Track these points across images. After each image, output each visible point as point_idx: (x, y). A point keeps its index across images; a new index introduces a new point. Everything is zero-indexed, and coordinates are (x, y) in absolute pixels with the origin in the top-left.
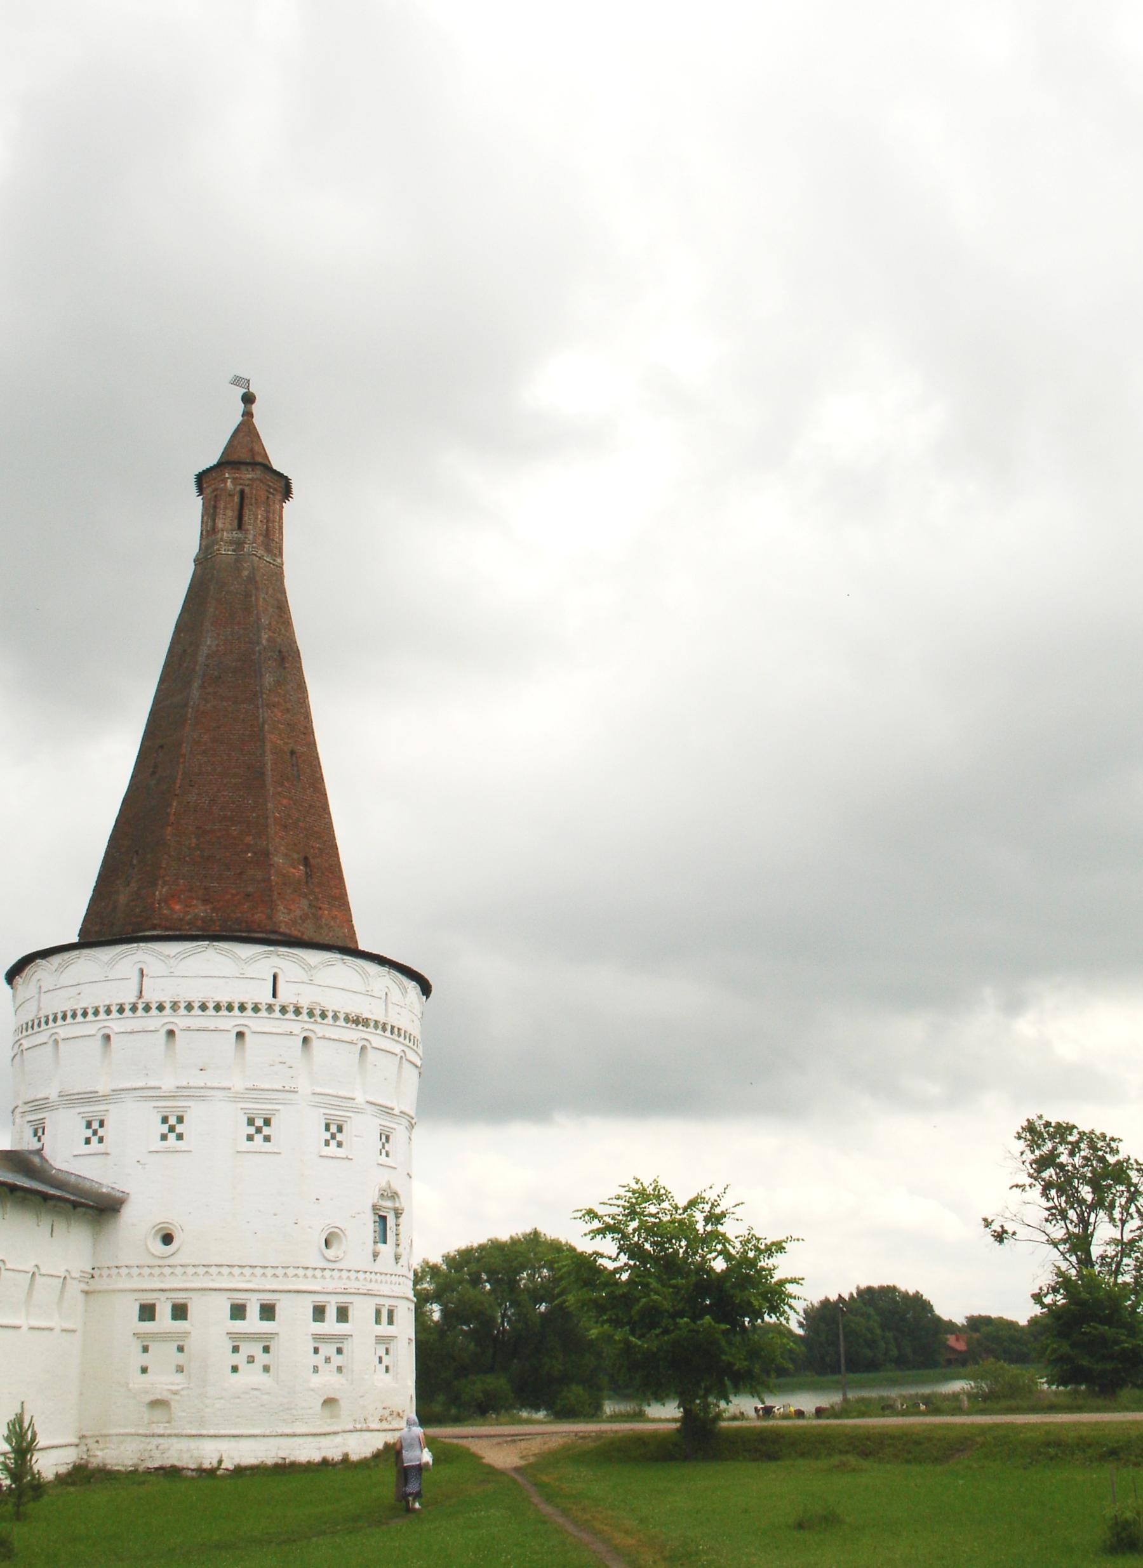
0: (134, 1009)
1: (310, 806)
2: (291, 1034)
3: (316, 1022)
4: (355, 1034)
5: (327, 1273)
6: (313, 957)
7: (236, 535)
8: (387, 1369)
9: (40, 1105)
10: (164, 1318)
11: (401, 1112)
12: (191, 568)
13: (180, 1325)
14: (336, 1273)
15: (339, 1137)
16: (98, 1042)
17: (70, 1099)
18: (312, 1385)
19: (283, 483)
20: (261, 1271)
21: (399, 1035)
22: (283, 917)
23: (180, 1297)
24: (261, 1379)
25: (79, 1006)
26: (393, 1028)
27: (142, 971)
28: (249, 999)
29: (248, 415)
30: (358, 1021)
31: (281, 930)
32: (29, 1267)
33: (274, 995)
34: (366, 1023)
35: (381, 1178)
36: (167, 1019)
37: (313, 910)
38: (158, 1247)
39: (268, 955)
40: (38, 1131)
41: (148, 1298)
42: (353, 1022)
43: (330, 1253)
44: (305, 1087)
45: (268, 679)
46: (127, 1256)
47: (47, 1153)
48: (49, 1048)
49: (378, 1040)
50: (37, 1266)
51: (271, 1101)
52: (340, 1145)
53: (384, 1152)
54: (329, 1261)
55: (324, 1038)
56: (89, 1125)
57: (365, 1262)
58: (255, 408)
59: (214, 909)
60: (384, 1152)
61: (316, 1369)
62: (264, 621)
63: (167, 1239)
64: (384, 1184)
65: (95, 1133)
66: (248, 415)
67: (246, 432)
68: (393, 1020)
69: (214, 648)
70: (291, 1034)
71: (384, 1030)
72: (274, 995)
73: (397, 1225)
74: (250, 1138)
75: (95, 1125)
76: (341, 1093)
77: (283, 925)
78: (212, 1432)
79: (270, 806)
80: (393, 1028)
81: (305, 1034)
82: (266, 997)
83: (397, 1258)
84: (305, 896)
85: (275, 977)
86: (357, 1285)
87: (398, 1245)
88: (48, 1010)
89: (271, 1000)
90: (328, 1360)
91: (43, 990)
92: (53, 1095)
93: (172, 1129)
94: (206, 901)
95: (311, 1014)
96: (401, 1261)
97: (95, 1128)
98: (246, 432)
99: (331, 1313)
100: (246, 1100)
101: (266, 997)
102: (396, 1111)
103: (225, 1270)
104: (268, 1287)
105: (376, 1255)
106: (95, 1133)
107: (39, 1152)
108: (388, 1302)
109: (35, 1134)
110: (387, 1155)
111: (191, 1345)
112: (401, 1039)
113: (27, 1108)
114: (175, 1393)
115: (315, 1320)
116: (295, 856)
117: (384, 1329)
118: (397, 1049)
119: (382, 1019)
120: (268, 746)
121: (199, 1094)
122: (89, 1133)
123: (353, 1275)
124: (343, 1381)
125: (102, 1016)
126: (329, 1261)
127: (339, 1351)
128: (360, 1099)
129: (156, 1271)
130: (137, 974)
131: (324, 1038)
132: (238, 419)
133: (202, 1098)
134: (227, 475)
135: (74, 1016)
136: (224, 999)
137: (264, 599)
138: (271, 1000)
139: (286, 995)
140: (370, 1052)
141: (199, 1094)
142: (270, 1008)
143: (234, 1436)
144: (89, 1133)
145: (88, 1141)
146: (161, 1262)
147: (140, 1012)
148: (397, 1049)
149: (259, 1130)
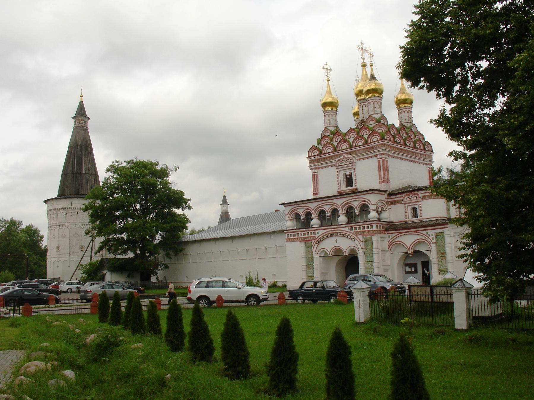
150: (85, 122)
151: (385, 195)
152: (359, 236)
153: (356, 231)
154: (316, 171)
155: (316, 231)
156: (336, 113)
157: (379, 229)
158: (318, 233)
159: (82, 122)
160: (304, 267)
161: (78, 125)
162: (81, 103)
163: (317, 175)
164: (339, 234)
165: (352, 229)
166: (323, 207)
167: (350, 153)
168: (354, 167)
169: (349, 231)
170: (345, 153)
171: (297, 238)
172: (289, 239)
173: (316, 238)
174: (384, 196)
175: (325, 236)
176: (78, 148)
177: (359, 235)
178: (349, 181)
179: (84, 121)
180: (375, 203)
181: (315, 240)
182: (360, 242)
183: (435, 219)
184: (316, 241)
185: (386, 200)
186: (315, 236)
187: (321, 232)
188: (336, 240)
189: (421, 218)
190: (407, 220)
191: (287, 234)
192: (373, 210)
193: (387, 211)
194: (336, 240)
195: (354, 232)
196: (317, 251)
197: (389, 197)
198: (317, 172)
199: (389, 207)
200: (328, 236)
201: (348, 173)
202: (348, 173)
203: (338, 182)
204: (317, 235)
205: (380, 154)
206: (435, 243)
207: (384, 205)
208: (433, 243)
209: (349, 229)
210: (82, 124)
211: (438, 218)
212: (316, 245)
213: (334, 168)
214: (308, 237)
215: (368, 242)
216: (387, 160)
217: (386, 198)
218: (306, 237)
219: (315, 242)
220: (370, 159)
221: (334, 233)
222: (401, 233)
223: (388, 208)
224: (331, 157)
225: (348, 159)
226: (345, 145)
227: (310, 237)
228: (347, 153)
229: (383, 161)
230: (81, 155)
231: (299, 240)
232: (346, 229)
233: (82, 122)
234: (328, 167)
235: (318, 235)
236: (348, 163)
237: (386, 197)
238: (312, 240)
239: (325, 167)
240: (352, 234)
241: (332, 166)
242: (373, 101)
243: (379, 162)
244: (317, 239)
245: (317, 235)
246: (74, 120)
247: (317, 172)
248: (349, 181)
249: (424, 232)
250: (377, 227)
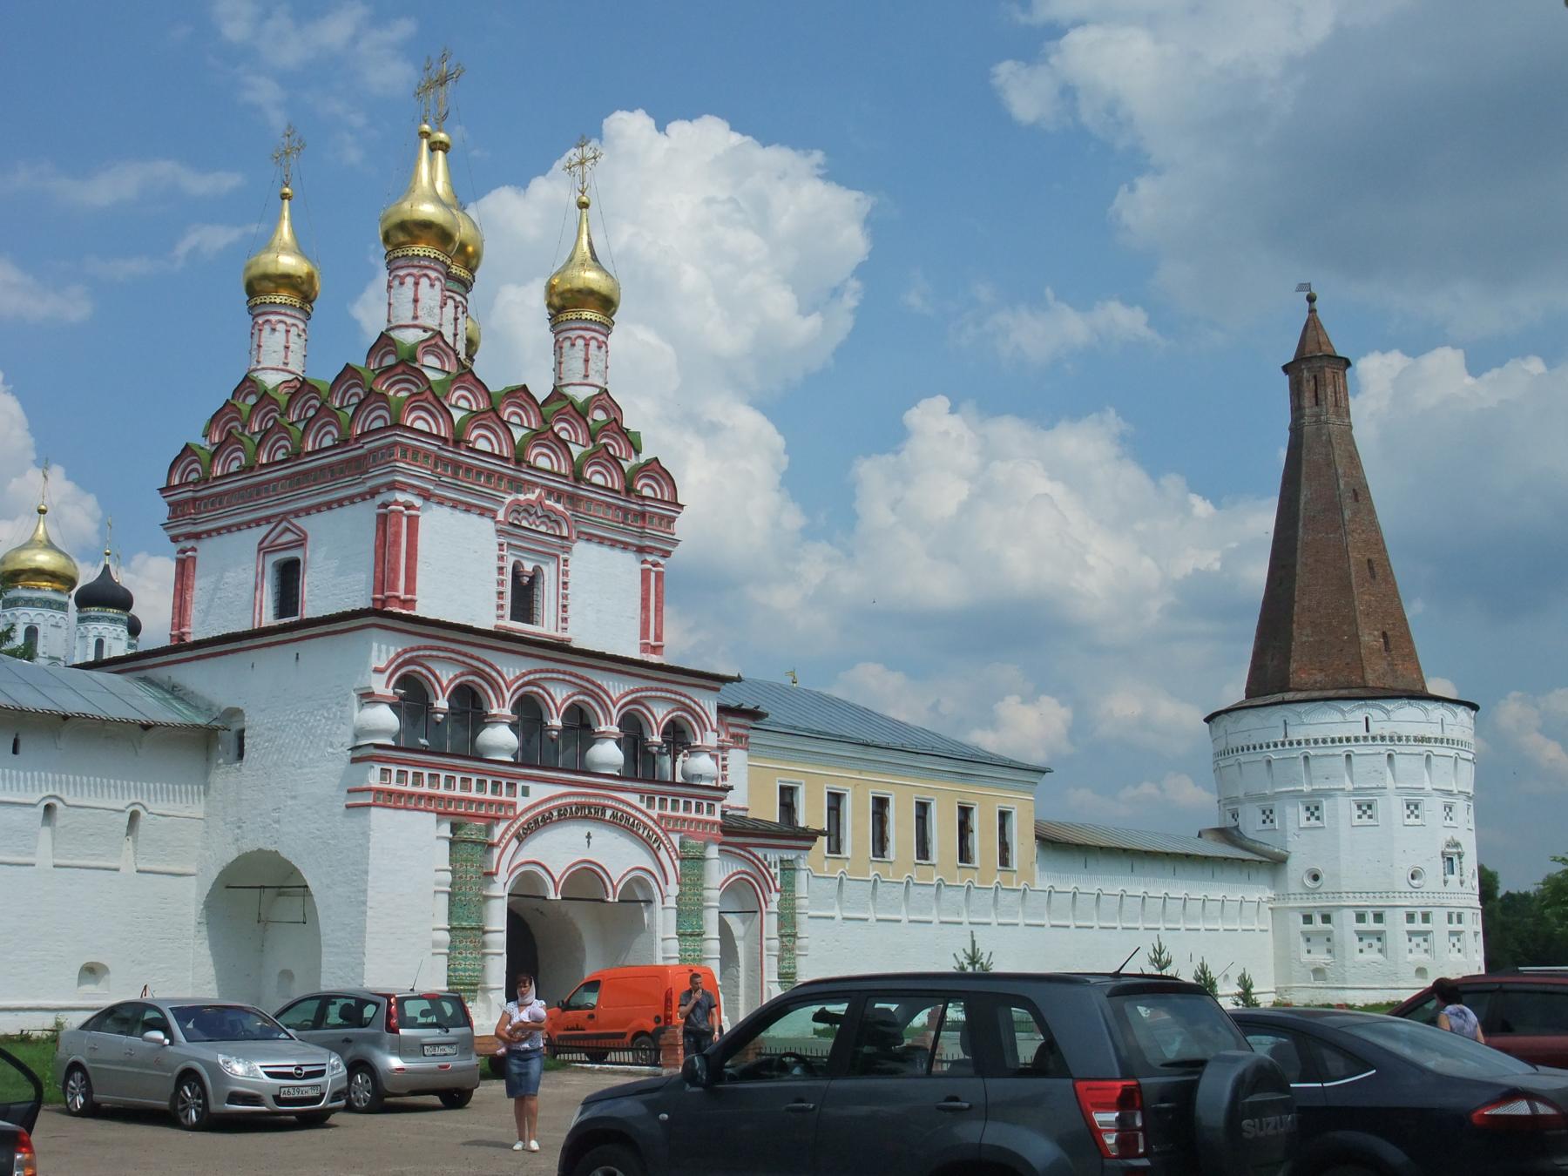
0: (1283, 744)
1: (1384, 595)
2: (1379, 754)
3: (1395, 744)
4: (1423, 749)
5: (1414, 895)
6: (1389, 705)
7: (1316, 409)
8: (1459, 951)
9: (1235, 801)
10: (1318, 923)
11: (1459, 792)
12: (1288, 434)
13: (1328, 926)
14: (1419, 895)
15: (1416, 812)
16: (1264, 765)
17: (1250, 798)
18: (1408, 960)
19: (1343, 362)
20: (1372, 895)
21: (1453, 744)
22: (1371, 679)
23: (1326, 911)
24: (1379, 957)
25: (1251, 744)
26: (1448, 740)
27: (1285, 721)
28: (1351, 735)
29: (1312, 311)
30: (1423, 740)
31: (1370, 685)
32: (1239, 897)
33: (1368, 730)
34: (1429, 740)
35: (1448, 835)
36: (1304, 749)
37: (1391, 667)
38: (1309, 883)
39: (1360, 707)
40: (1235, 816)
41: (1307, 912)
42: (1419, 741)
43: (1415, 882)
44: (1389, 782)
45: (1347, 514)
46: (1294, 887)
47: (1241, 828)
48: (1236, 768)
49: (1437, 750)
50: (1243, 897)
51: (1371, 795)
52: (1417, 817)
53: (1448, 818)
54: (1413, 887)
55: (1401, 754)
56: (1264, 812)
57: (1439, 887)
58: (1317, 304)
59: (1326, 676)
60: (1448, 818)
61: (1411, 951)
62: (1340, 471)
63: (1316, 878)
64: (1449, 838)
65: (1268, 817)
66: (1312, 311)
67: (1312, 326)
68: (1448, 734)
69: (1309, 496)
70: (1379, 754)
71: (1442, 743)
72: (1368, 730)
73: (1461, 863)
74: (1360, 817)
75: (1268, 813)
76: (1414, 786)
77: (1371, 682)
78: (1349, 986)
79: (1356, 603)
80: (1448, 740)
81: (1389, 752)
82: (1363, 733)
83: (1462, 883)
84: (1385, 658)
85: (1367, 719)
86: (1435, 901)
87: (1461, 875)
88: (1233, 744)
89: (1365, 734)
90: (1418, 945)
91: (1228, 732)
92: (1241, 794)
93: (1312, 814)
94: (1321, 670)
95: (1391, 739)
96: (1465, 885)
97: (1268, 815)
98: (1312, 326)
99: (1418, 917)
100: (1355, 795)
101: (1363, 733)
102: (1456, 792)
103: (1351, 895)
104: (1378, 904)
105: (1445, 882)
106: (1268, 817)
107: (1237, 828)
108: (1456, 911)
109: (1233, 816)
110: (1451, 819)
111: (1336, 938)
112: (1455, 746)
113: (1227, 801)
114: (1326, 964)
115: (1408, 922)
116: (1376, 633)
117: (1455, 926)
118: (1452, 753)
119: (1439, 736)
120: (1352, 561)
121: (1327, 794)
122: (1264, 817)
123: (1431, 895)
124: (1429, 957)
125: (1265, 749)
126: (1413, 887)
127: (1425, 940)
128: (1428, 787)
129: (1311, 897)
130: (1283, 723)
131: (1401, 754)
132: (1306, 315)
133: (1331, 796)
134: (1303, 367)
135: (1248, 749)
136: (1336, 736)
137: (1339, 455)
138: (1365, 734)
139: (1375, 729)
140: (1434, 759)
141: (1327, 794)
142: (1365, 738)
143: (1363, 989)
144: (1264, 817)
145: (1264, 822)
146: (1312, 891)
147: (1287, 747)
148: (1452, 753)
149: (1365, 812)
152: (672, 836)
153: (664, 812)
154: (418, 502)
155: (520, 785)
156: (607, 336)
158: (526, 792)
160: (446, 937)
163: (413, 522)
164: (609, 813)
165: (651, 801)
166: (547, 685)
167: (560, 496)
168: (562, 556)
169: (643, 806)
170: (543, 487)
171: (430, 798)
172: (390, 793)
173: (518, 811)
175: (555, 814)
177: (672, 831)
178: (524, 596)
181: (516, 818)
182: (674, 857)
184: (516, 826)
186: (513, 805)
187: (540, 792)
188: (589, 836)
191: (378, 767)
194: (589, 836)
195: (661, 817)
198: (418, 509)
200: (566, 815)
201: (528, 567)
202: (528, 567)
203: (501, 589)
204: (522, 803)
205: (661, 550)
208: (777, 891)
209: (642, 800)
212: (514, 843)
213: (487, 525)
214: (480, 803)
215: (693, 862)
218: (470, 801)
219: (513, 830)
220: (617, 555)
221: (590, 806)
224: (490, 474)
225: (550, 517)
226: (549, 457)
227: (490, 803)
228: (550, 492)
229: (659, 576)
231: (441, 809)
232: (634, 799)
234: (468, 508)
236: (543, 528)
238: (498, 819)
239: (455, 505)
240: (651, 823)
241: (483, 512)
242: (588, 334)
243: (645, 574)
244: (523, 820)
245: (522, 803)
247: (418, 509)
248: (524, 596)
249: (760, 853)
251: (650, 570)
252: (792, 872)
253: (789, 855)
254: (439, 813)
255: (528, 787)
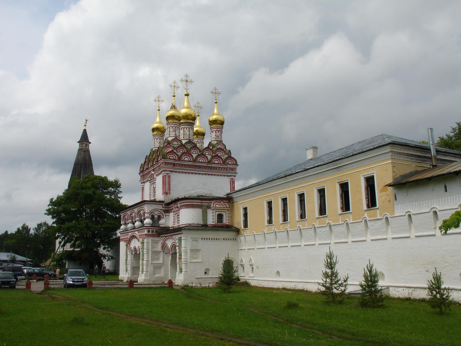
150: (86, 145)
151: (162, 205)
157: (151, 233)
159: (83, 145)
161: (81, 148)
162: (85, 130)
174: (162, 205)
176: (79, 165)
179: (85, 145)
180: (149, 212)
183: (185, 225)
185: (164, 209)
189: (178, 224)
190: (175, 225)
192: (147, 217)
193: (164, 218)
195: (139, 235)
196: (129, 249)
197: (167, 207)
199: (167, 214)
206: (178, 246)
207: (161, 213)
210: (83, 147)
211: (187, 225)
216: (170, 176)
217: (163, 207)
222: (166, 237)
223: (166, 216)
230: (81, 171)
233: (83, 145)
235: (129, 236)
237: (164, 206)
246: (79, 144)
250: (149, 231)
251: (166, 175)
252: (180, 240)
253: (179, 236)
254: (124, 241)
255: (148, 232)
